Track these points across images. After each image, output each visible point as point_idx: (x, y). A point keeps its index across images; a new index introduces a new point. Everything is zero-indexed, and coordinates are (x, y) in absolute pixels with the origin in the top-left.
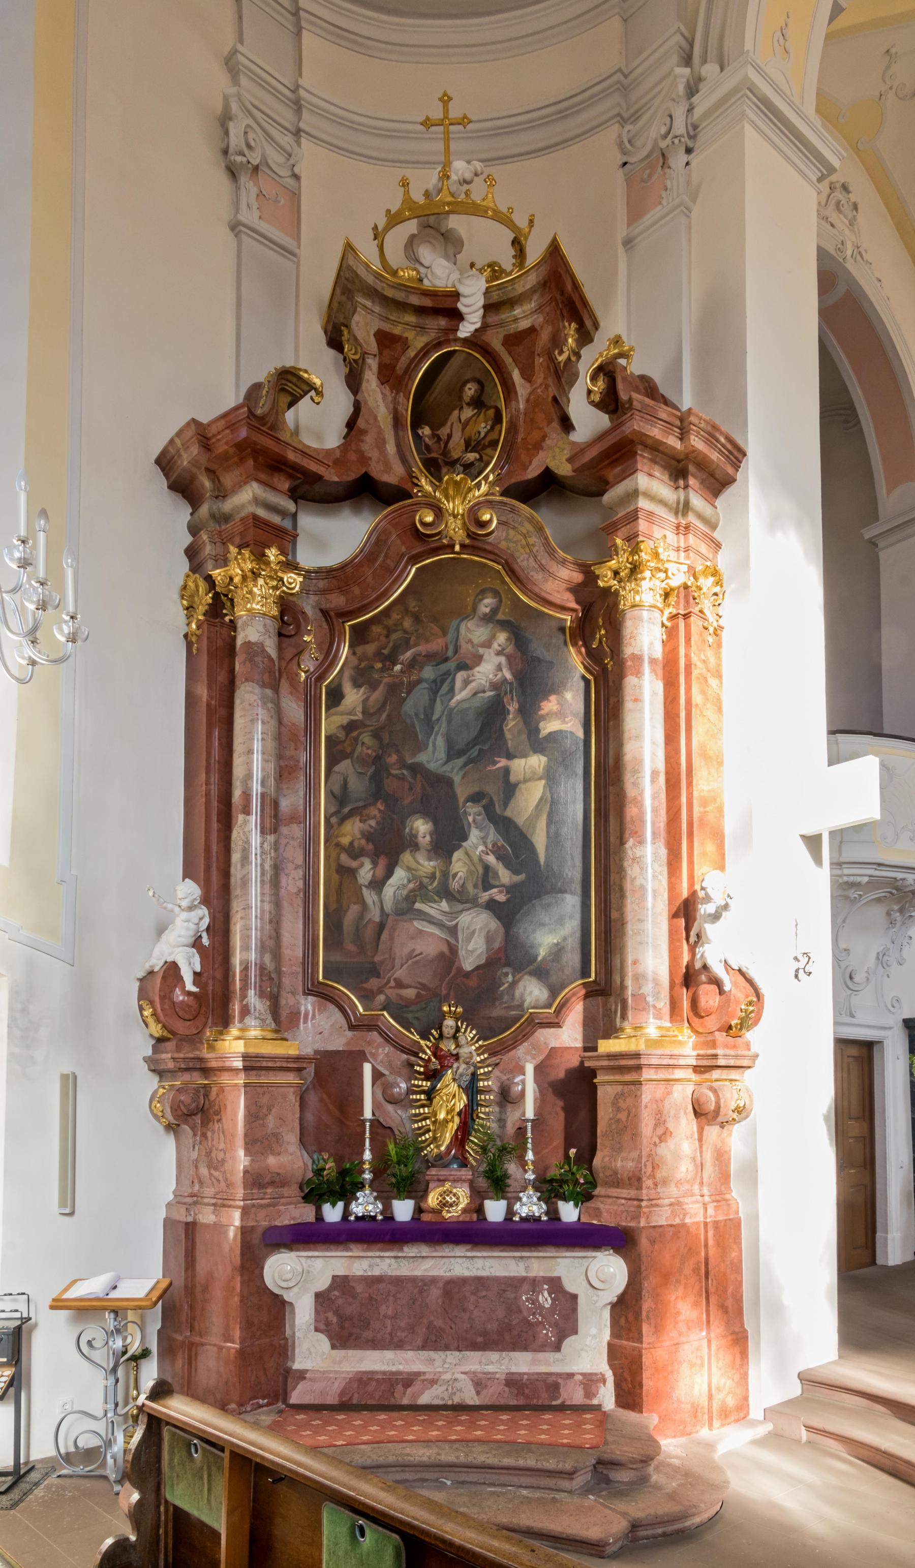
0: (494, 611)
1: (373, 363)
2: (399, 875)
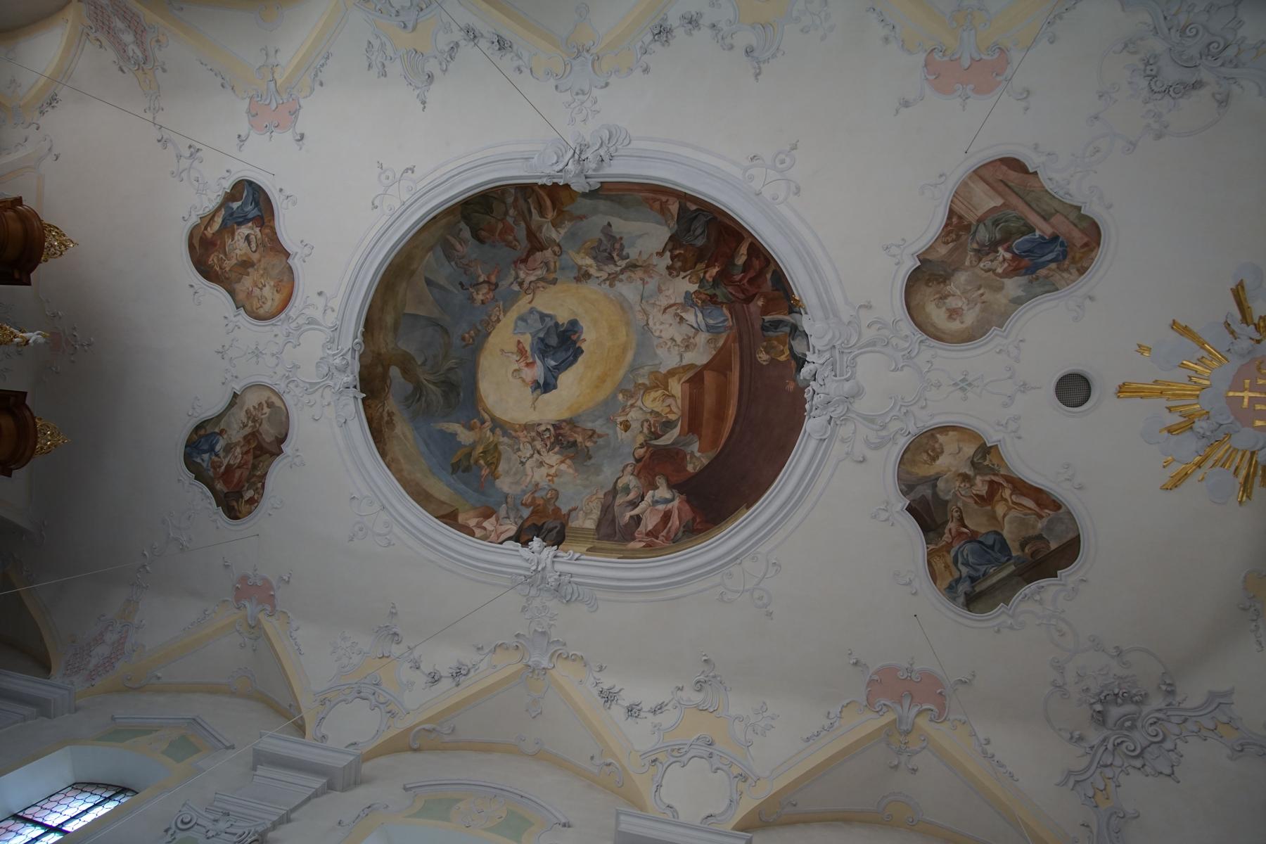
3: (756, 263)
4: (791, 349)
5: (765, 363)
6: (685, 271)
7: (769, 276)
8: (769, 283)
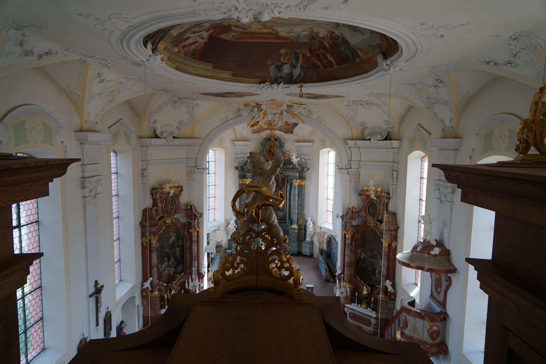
0: (174, 231)
1: (159, 200)
2: (164, 265)
3: (325, 61)
4: (286, 63)
5: (280, 52)
6: (330, 36)
7: (319, 63)
8: (316, 62)
